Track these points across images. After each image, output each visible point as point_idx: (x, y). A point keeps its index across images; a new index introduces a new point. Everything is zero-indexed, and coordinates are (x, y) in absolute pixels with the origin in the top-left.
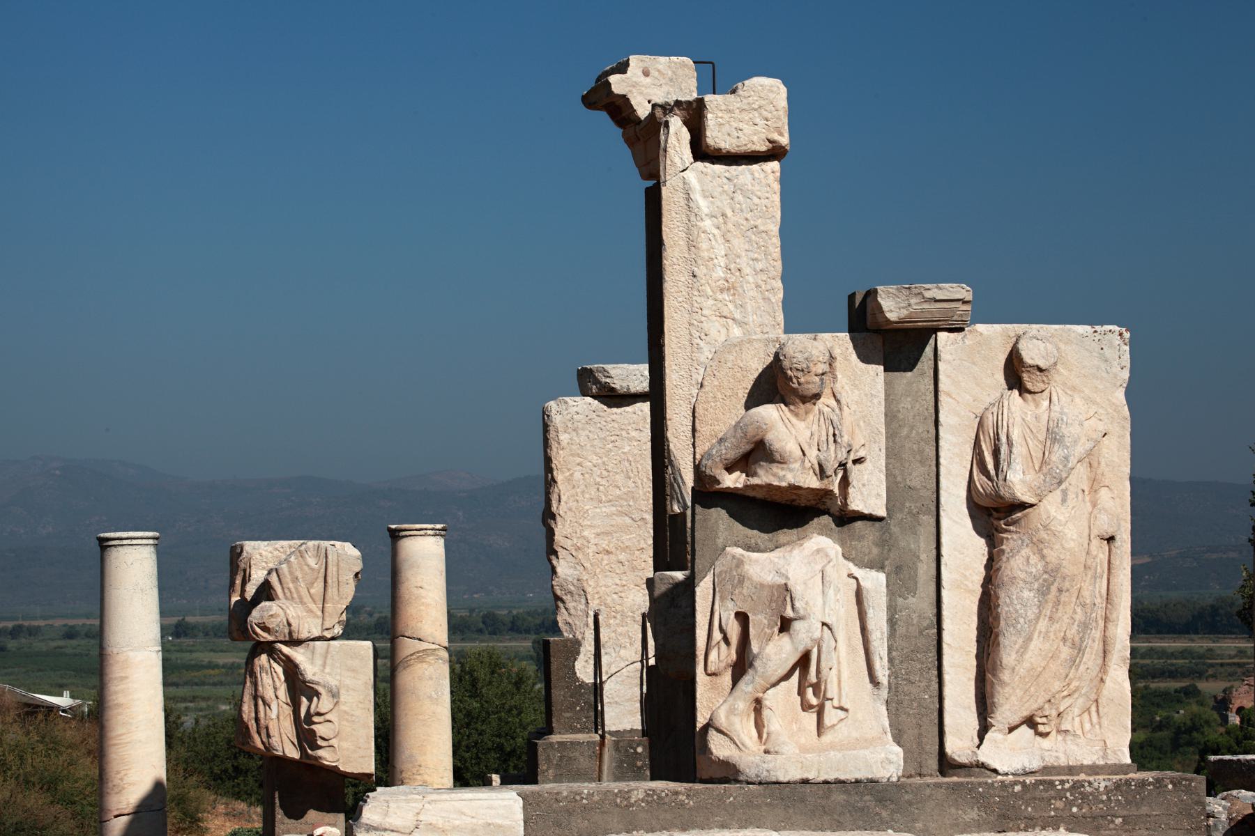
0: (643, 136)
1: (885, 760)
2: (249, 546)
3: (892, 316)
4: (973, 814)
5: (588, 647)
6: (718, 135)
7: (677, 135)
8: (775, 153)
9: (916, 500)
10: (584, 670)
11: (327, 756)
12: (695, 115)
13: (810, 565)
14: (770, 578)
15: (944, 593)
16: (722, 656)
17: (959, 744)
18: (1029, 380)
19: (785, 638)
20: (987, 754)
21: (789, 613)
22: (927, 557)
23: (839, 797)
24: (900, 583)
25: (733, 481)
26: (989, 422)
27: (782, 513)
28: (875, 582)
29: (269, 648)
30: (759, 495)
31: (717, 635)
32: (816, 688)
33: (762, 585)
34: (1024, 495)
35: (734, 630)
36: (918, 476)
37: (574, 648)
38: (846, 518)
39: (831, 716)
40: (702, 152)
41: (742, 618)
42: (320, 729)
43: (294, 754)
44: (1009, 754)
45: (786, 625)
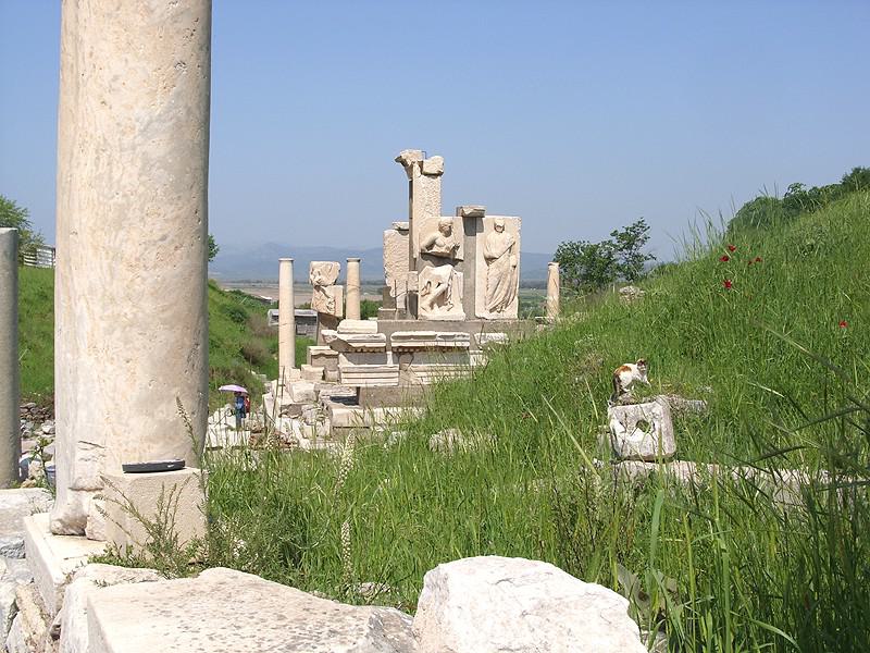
0: (409, 169)
2: (314, 263)
5: (393, 288)
6: (425, 170)
7: (416, 168)
8: (440, 174)
9: (471, 256)
10: (392, 294)
12: (421, 165)
13: (446, 270)
23: (451, 324)
28: (460, 274)
37: (390, 288)
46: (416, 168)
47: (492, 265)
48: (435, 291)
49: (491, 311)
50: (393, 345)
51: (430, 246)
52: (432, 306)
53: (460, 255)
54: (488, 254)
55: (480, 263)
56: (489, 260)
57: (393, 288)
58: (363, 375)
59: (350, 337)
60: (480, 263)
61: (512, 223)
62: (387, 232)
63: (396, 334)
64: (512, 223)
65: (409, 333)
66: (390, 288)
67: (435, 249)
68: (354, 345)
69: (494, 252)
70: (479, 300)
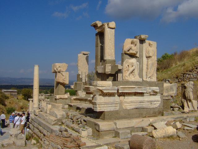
1: (140, 80)
2: (57, 64)
3: (142, 38)
4: (148, 85)
7: (106, 26)
9: (141, 56)
10: (81, 77)
12: (108, 25)
14: (131, 62)
17: (145, 79)
20: (147, 80)
21: (133, 65)
22: (142, 61)
24: (140, 64)
27: (132, 56)
28: (138, 63)
33: (130, 63)
34: (151, 56)
36: (141, 54)
37: (80, 75)
44: (148, 80)
45: (133, 66)
46: (106, 26)
47: (150, 59)
48: (131, 69)
49: (149, 78)
50: (120, 91)
51: (128, 51)
52: (129, 75)
53: (138, 55)
54: (148, 55)
55: (145, 59)
56: (148, 57)
57: (81, 75)
59: (104, 88)
60: (145, 59)
61: (154, 44)
62: (79, 55)
63: (121, 87)
64: (154, 44)
65: (126, 87)
66: (80, 75)
67: (131, 52)
68: (105, 91)
69: (151, 55)
70: (144, 74)
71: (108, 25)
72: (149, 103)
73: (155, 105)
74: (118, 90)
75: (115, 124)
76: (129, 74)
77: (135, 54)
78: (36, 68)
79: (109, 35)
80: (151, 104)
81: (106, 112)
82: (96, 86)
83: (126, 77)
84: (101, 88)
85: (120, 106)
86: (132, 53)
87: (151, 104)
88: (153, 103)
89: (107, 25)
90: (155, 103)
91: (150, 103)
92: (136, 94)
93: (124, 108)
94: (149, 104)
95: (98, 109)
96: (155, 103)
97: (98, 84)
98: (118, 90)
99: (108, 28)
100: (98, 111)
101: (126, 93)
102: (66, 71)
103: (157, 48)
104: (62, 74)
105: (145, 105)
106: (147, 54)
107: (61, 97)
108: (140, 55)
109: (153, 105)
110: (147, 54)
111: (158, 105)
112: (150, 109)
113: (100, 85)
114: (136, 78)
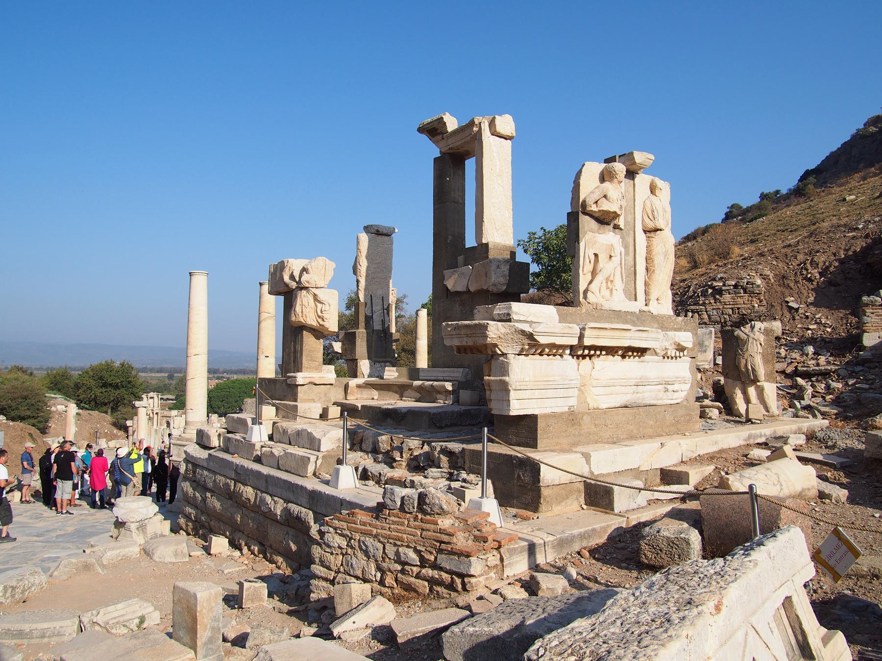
2: (291, 260)
4: (656, 325)
11: (326, 324)
15: (637, 256)
16: (589, 267)
18: (657, 192)
19: (611, 263)
25: (594, 208)
26: (648, 203)
29: (306, 288)
30: (596, 215)
31: (587, 261)
32: (612, 281)
34: (662, 227)
35: (593, 258)
38: (616, 227)
39: (614, 291)
40: (495, 133)
41: (596, 255)
42: (325, 316)
43: (315, 324)
50: (587, 342)
53: (621, 222)
54: (650, 225)
58: (537, 394)
60: (641, 237)
68: (542, 340)
71: (492, 124)
72: (660, 387)
73: (676, 395)
74: (581, 337)
75: (587, 457)
76: (599, 284)
77: (616, 215)
78: (200, 283)
79: (497, 159)
80: (667, 390)
81: (546, 416)
82: (510, 320)
83: (589, 294)
84: (527, 328)
85: (578, 397)
86: (607, 213)
87: (667, 390)
88: (670, 387)
89: (487, 124)
90: (676, 387)
91: (662, 386)
92: (628, 352)
93: (591, 406)
94: (659, 391)
95: (517, 407)
96: (676, 387)
97: (517, 314)
98: (581, 337)
99: (492, 134)
100: (513, 412)
101: (601, 348)
102: (330, 286)
103: (671, 203)
104: (315, 295)
105: (648, 395)
106: (647, 220)
107: (312, 380)
108: (626, 222)
109: (669, 394)
110: (647, 220)
111: (684, 394)
112: (663, 409)
113: (522, 318)
114: (619, 302)
